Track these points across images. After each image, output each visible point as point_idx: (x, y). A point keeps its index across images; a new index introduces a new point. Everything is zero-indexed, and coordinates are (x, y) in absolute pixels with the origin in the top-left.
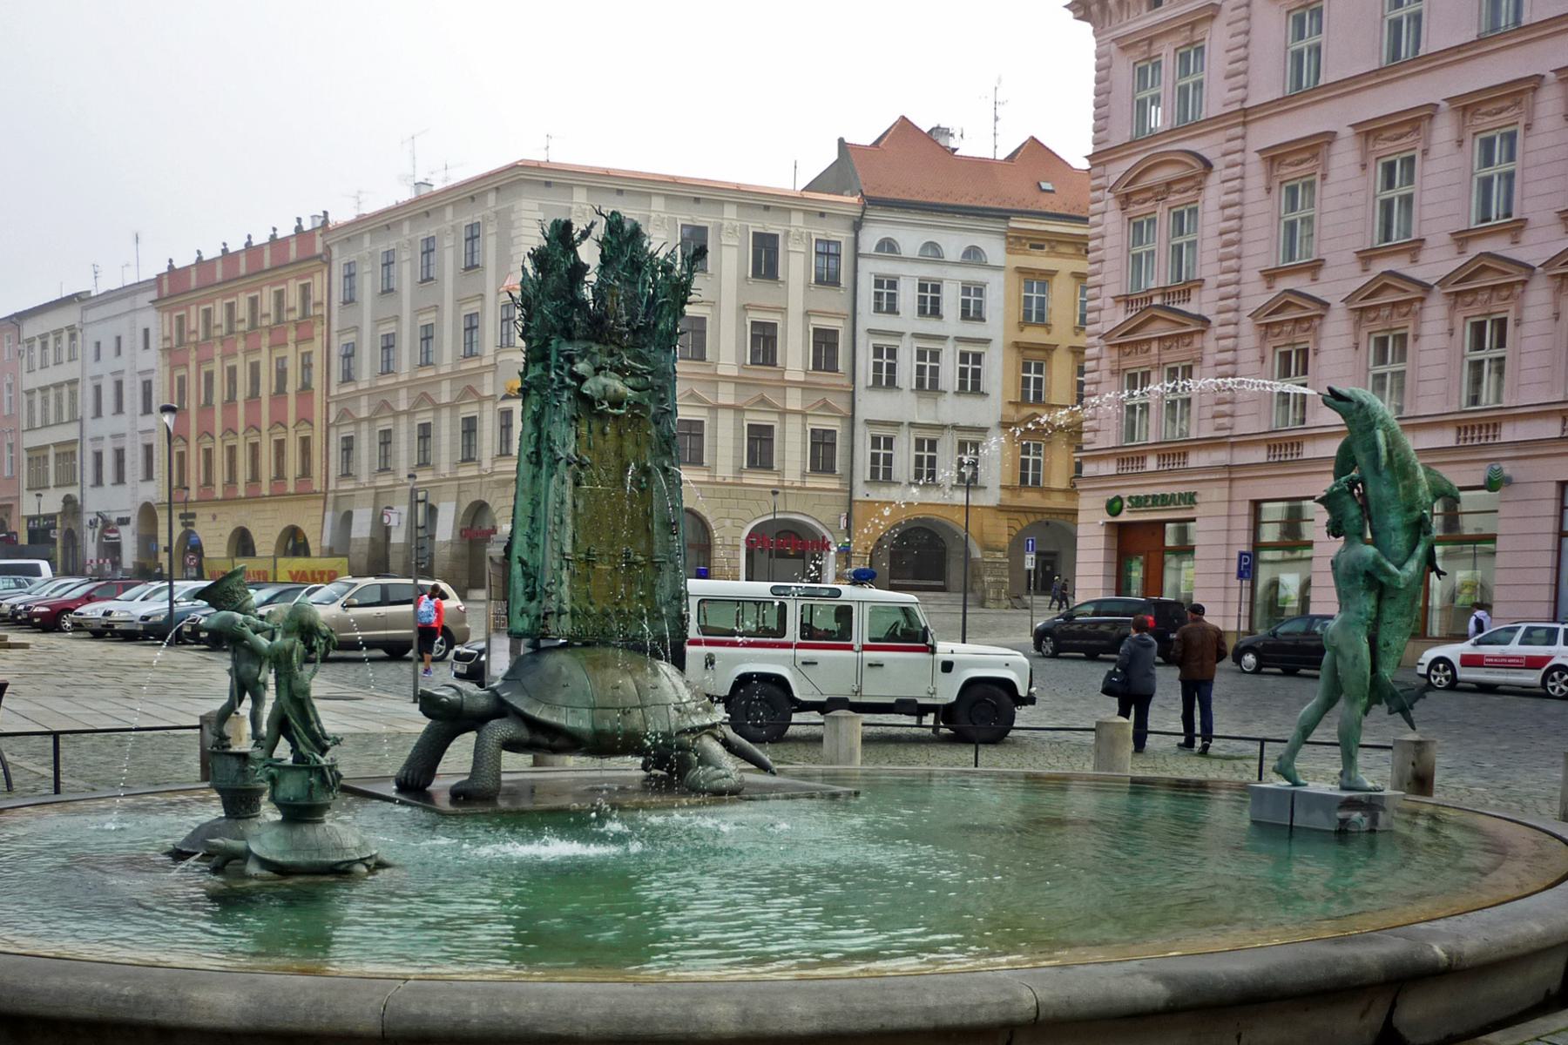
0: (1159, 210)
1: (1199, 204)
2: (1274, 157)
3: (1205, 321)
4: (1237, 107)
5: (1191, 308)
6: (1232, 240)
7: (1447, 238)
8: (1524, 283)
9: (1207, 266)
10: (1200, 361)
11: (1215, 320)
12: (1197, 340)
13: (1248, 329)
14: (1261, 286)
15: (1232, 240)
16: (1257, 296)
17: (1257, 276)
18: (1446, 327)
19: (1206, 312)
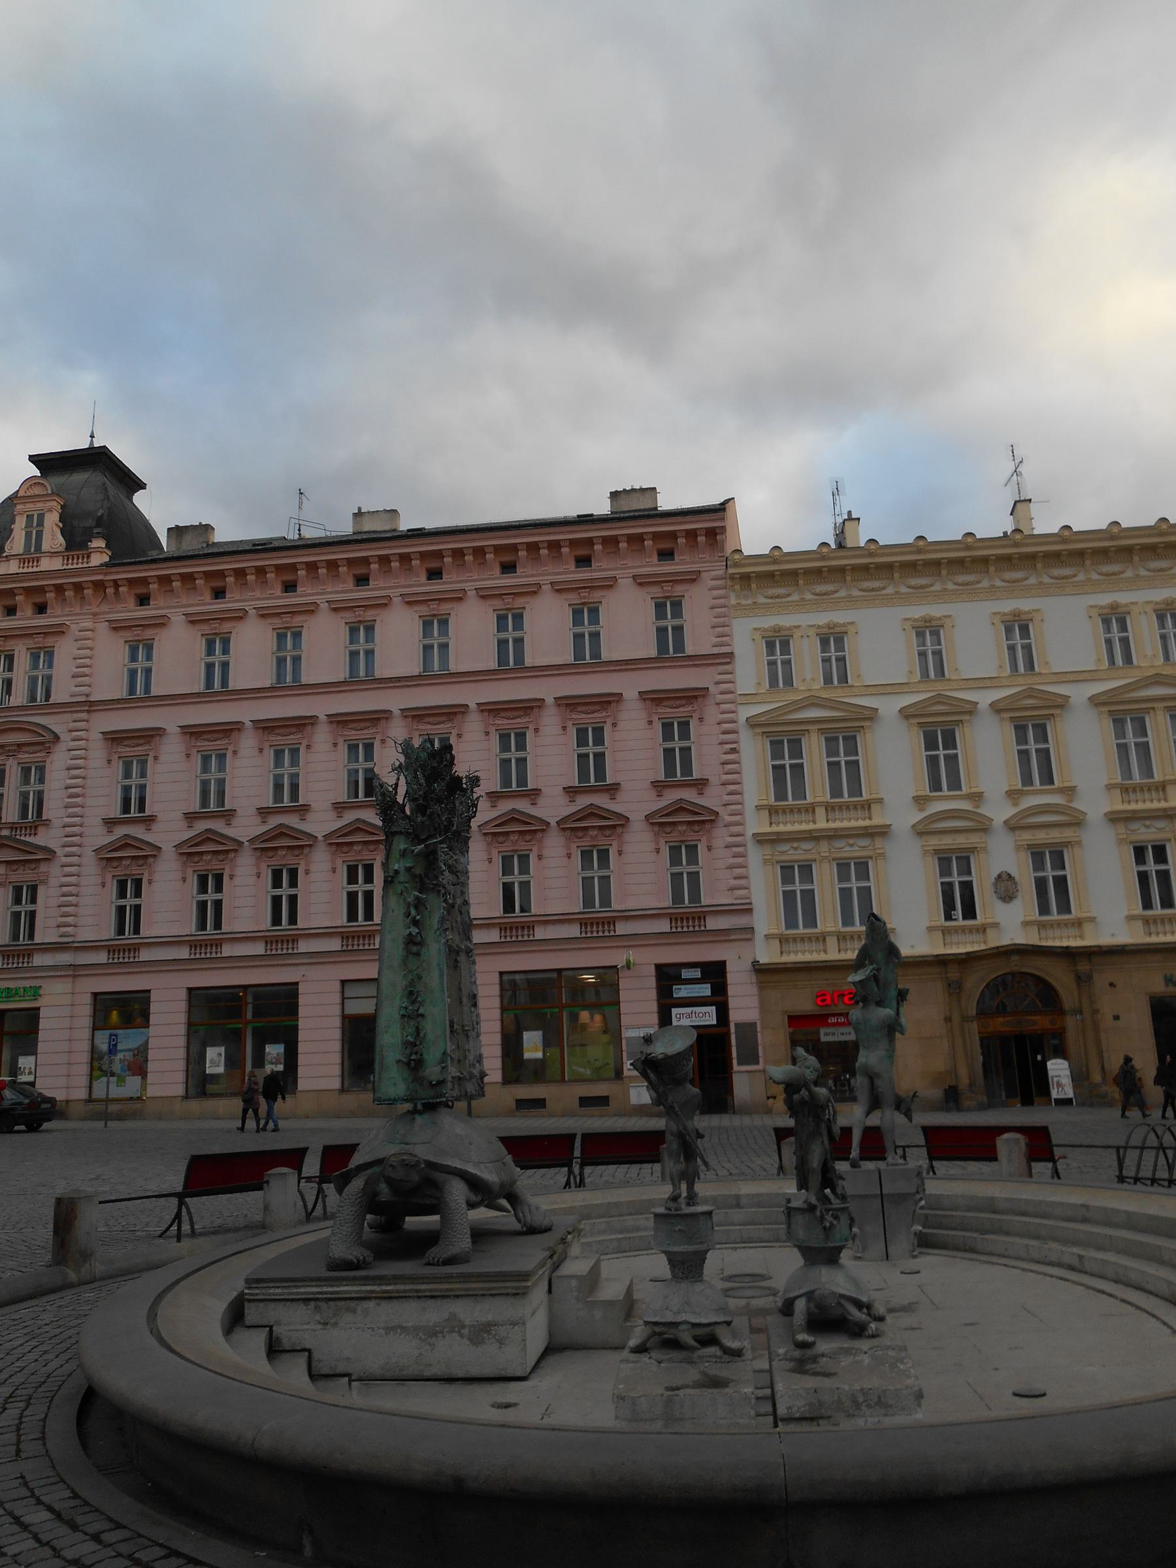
0: (8, 763)
1: (48, 762)
2: (114, 738)
3: (52, 852)
4: (83, 699)
5: (40, 839)
6: (75, 793)
7: (253, 811)
8: (310, 846)
9: (53, 809)
10: (45, 882)
11: (59, 852)
12: (43, 867)
13: (89, 859)
14: (102, 830)
15: (75, 793)
16: (99, 837)
17: (98, 821)
18: (255, 871)
19: (52, 845)
